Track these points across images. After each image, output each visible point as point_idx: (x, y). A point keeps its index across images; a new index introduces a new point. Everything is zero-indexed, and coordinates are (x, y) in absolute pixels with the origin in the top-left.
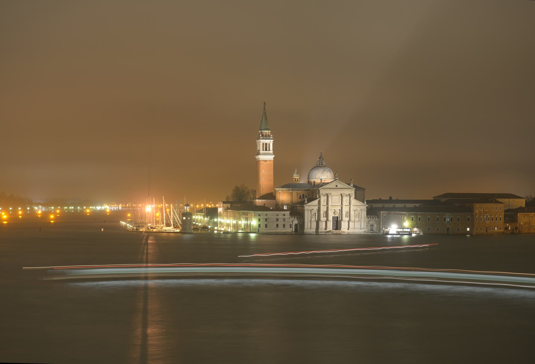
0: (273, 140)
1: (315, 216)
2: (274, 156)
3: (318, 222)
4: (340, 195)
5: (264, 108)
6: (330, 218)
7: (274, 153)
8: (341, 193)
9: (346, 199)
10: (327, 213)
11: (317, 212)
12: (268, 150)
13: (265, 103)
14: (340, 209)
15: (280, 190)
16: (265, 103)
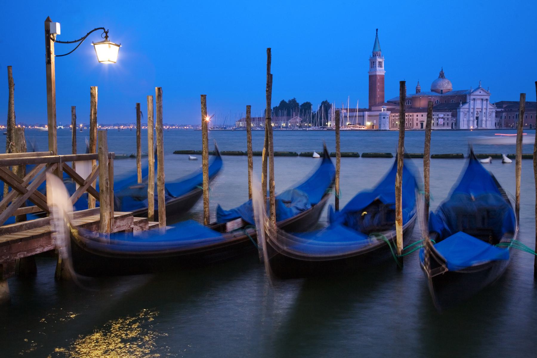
1: (466, 116)
2: (385, 72)
5: (377, 33)
6: (475, 118)
9: (485, 102)
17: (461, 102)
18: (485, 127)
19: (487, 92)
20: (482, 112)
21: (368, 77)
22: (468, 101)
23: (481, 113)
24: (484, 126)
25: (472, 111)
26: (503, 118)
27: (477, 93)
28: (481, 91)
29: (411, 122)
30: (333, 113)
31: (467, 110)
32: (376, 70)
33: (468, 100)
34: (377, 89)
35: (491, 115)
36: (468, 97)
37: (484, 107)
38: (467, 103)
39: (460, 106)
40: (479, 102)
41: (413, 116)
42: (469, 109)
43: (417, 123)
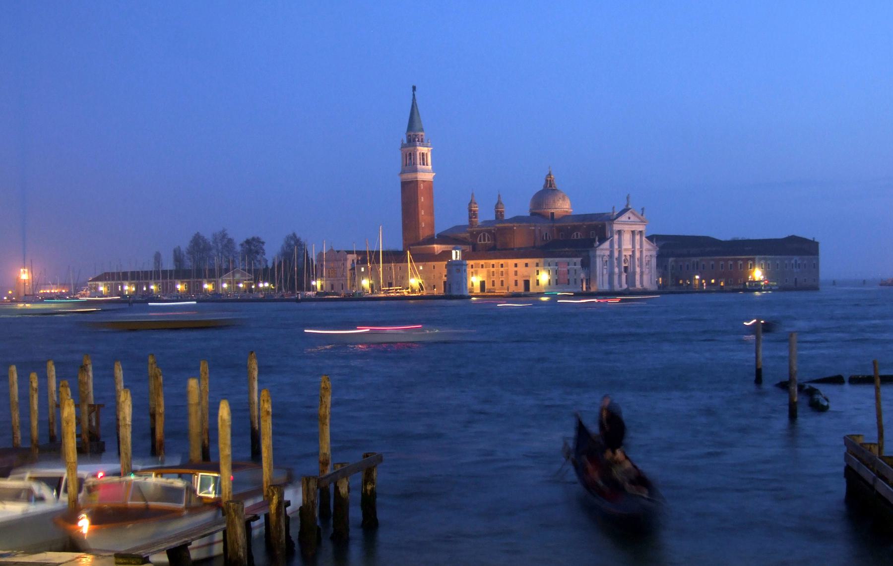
0: (431, 148)
1: (607, 265)
3: (611, 275)
4: (631, 232)
5: (414, 95)
6: (623, 270)
7: (434, 169)
8: (633, 230)
9: (637, 237)
10: (619, 259)
11: (608, 260)
12: (425, 164)
13: (414, 88)
14: (631, 254)
15: (514, 226)
16: (414, 88)
17: (597, 239)
18: (641, 288)
19: (641, 217)
22: (609, 235)
24: (638, 285)
26: (670, 269)
27: (624, 218)
28: (631, 215)
29: (503, 279)
34: (420, 209)
35: (649, 263)
36: (608, 227)
37: (637, 246)
38: (608, 239)
39: (595, 245)
41: (507, 266)
43: (516, 281)
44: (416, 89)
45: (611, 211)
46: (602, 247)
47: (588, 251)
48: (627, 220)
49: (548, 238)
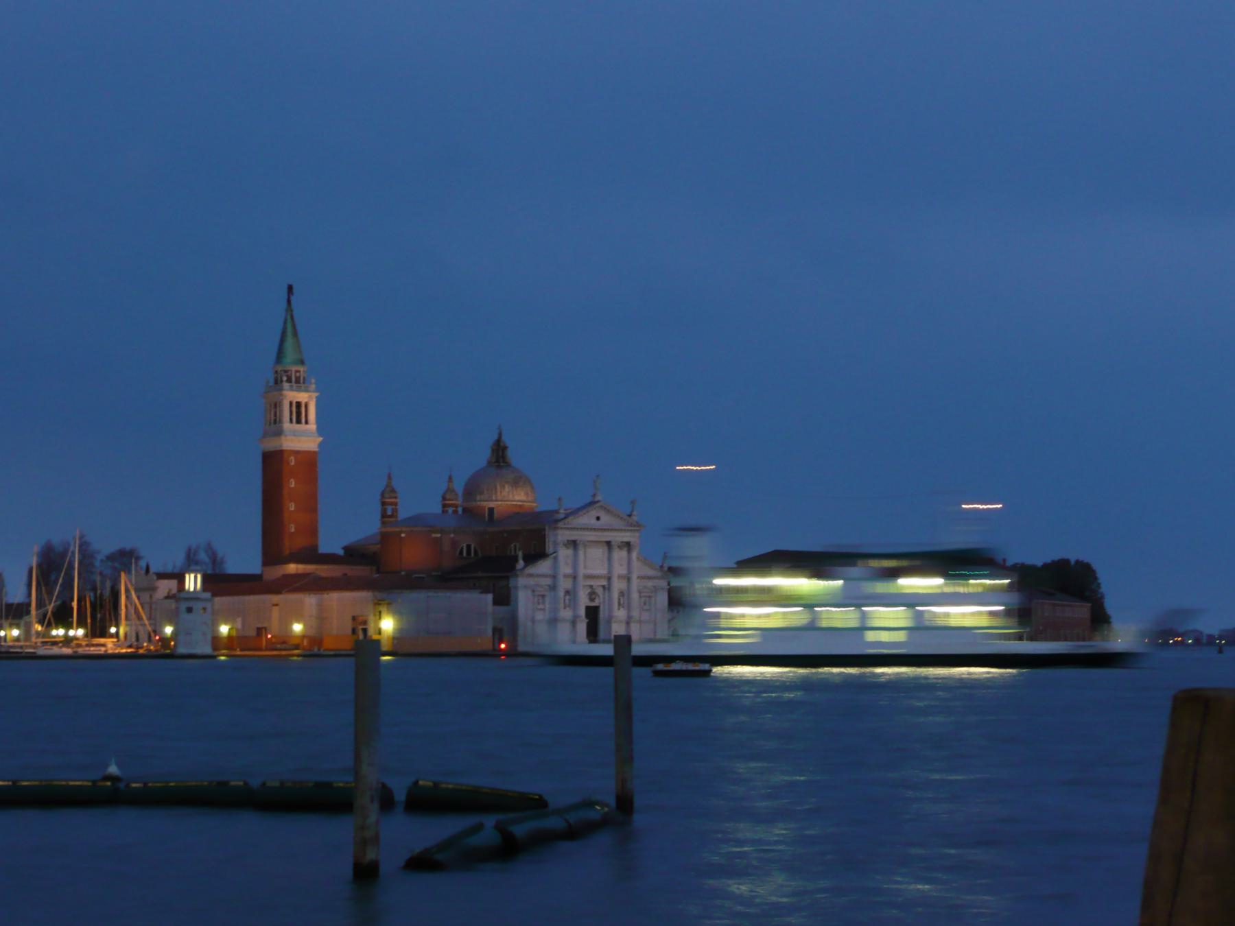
0: (316, 394)
1: (544, 603)
2: (321, 439)
5: (289, 301)
6: (582, 612)
7: (320, 430)
12: (303, 420)
13: (290, 288)
16: (290, 288)
17: (520, 554)
20: (609, 589)
21: (260, 460)
23: (607, 594)
25: (564, 584)
27: (587, 519)
28: (602, 514)
30: (127, 591)
31: (548, 581)
32: (279, 433)
33: (551, 546)
37: (619, 569)
40: (598, 553)
42: (554, 577)
44: (294, 290)
45: (554, 507)
46: (532, 570)
47: (507, 578)
48: (594, 521)
49: (472, 555)
